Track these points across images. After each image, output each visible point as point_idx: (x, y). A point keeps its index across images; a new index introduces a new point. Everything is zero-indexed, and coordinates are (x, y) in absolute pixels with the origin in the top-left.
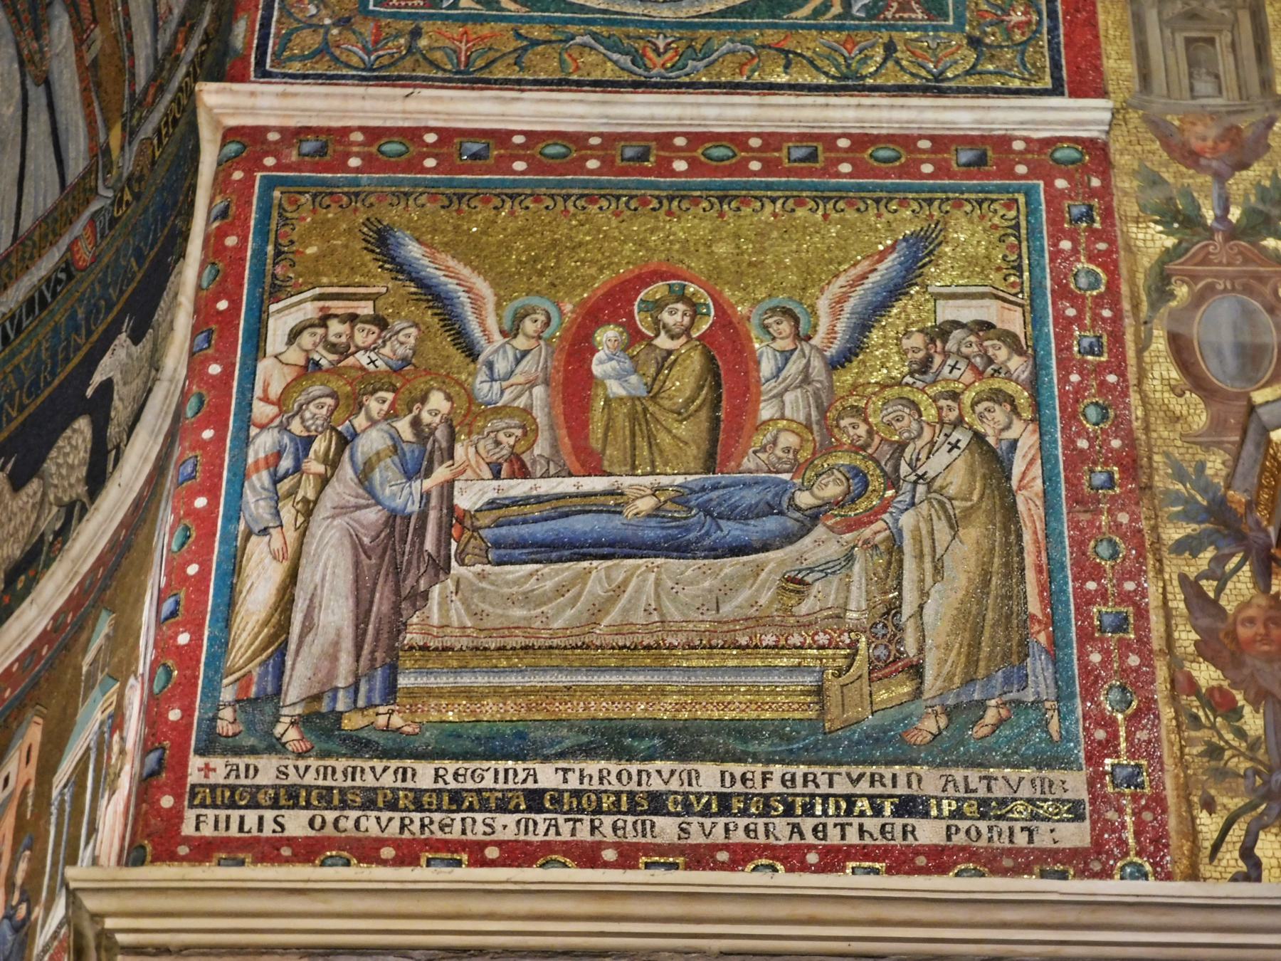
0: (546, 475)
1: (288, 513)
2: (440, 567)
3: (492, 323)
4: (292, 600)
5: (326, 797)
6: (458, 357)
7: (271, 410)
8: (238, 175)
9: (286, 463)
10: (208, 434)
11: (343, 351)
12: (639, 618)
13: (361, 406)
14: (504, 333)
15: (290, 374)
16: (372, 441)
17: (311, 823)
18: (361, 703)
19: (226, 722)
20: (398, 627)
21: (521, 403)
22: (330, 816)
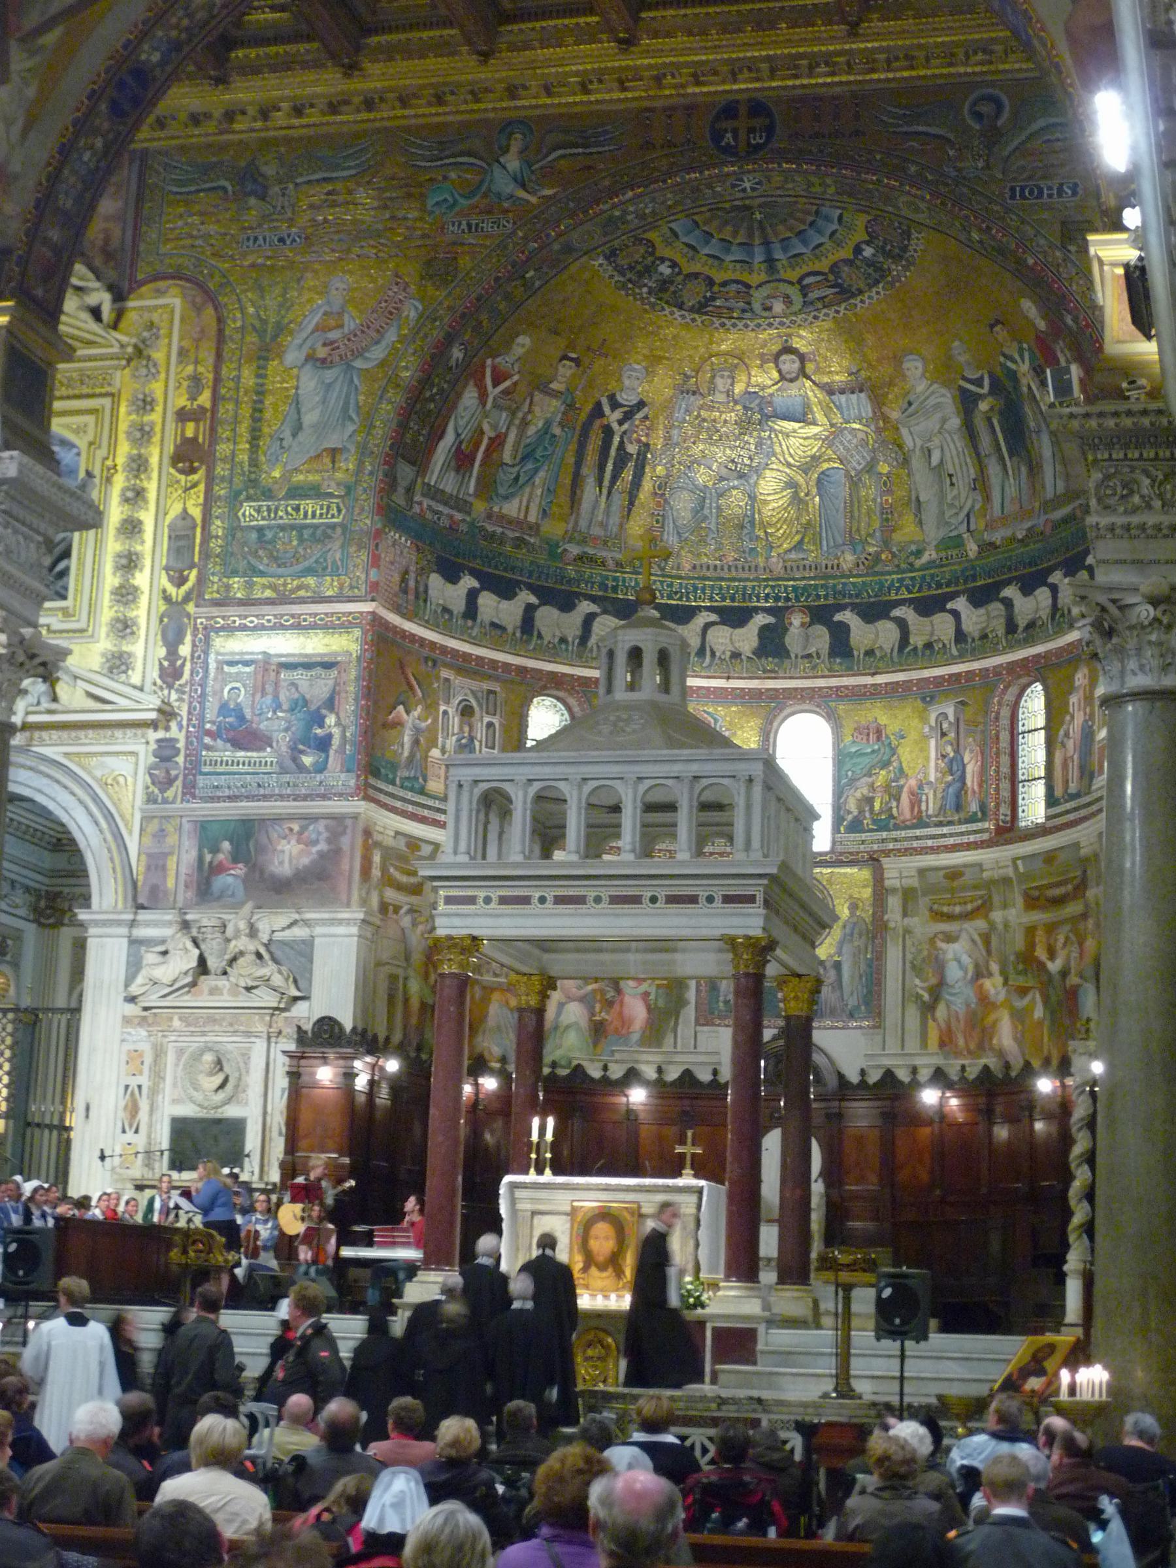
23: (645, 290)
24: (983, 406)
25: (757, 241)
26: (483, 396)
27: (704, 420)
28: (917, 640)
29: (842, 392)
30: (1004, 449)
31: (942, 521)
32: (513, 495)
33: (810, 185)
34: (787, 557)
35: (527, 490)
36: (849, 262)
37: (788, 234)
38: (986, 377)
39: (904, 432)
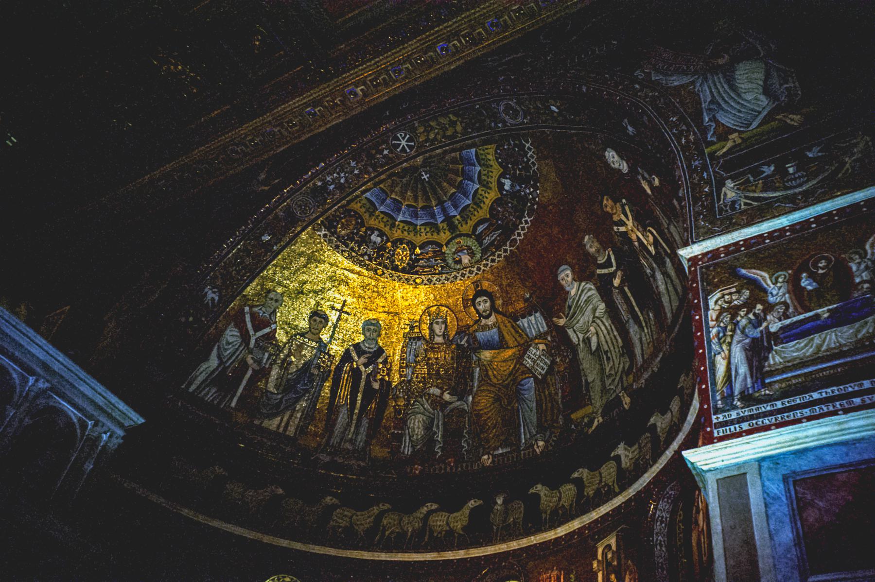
0: (794, 316)
1: (724, 347)
2: (770, 349)
3: (769, 282)
4: (731, 368)
5: (752, 417)
6: (762, 294)
7: (714, 323)
8: (693, 269)
9: (721, 335)
10: (699, 334)
11: (730, 302)
12: (833, 345)
13: (738, 314)
14: (773, 284)
15: (717, 313)
16: (744, 322)
17: (749, 425)
18: (756, 390)
19: (720, 404)
20: (761, 367)
21: (783, 300)
22: (754, 422)
23: (366, 257)
24: (616, 282)
25: (434, 203)
26: (245, 337)
27: (429, 359)
28: (590, 491)
29: (523, 317)
30: (637, 309)
31: (604, 390)
32: (275, 415)
33: (444, 129)
34: (496, 453)
35: (288, 413)
36: (497, 202)
37: (454, 190)
38: (611, 253)
39: (570, 332)
